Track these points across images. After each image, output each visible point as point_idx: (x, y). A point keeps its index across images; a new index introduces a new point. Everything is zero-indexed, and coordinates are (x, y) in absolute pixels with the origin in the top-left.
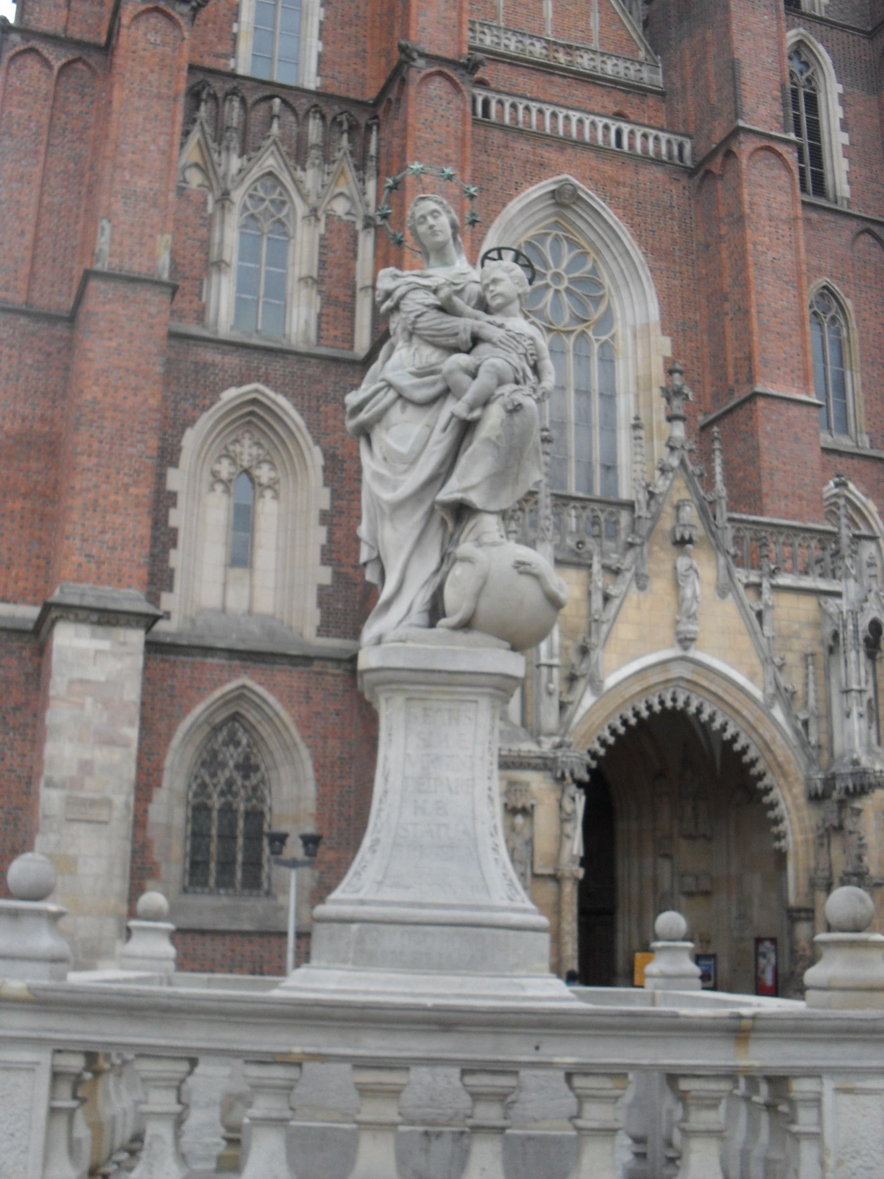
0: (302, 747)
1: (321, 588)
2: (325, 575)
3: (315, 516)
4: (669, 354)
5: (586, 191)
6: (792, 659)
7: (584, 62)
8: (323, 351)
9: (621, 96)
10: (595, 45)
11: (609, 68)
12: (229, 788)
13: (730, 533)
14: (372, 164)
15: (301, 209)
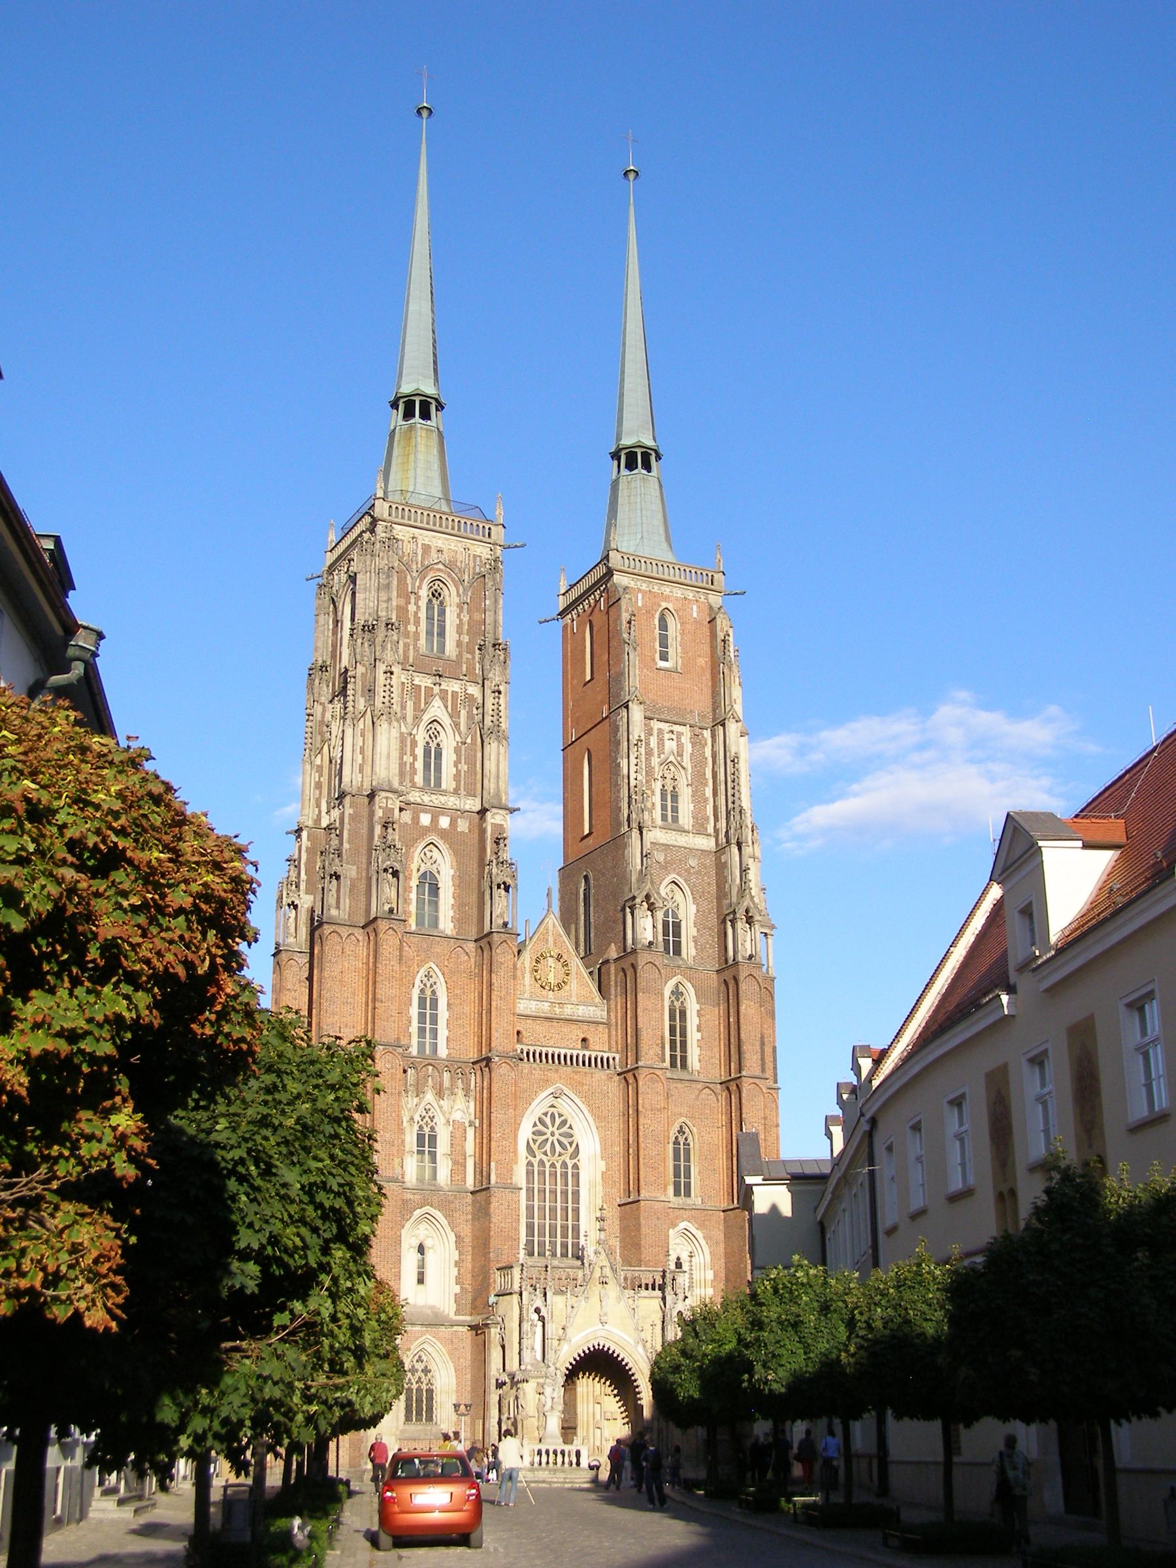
0: (450, 1362)
1: (456, 1295)
2: (457, 1289)
3: (453, 1263)
4: (604, 1170)
5: (566, 1091)
6: (648, 1328)
7: (568, 1011)
8: (454, 1188)
9: (585, 1027)
10: (574, 999)
11: (582, 1012)
12: (419, 1381)
13: (622, 1278)
14: (472, 1093)
15: (443, 1120)
